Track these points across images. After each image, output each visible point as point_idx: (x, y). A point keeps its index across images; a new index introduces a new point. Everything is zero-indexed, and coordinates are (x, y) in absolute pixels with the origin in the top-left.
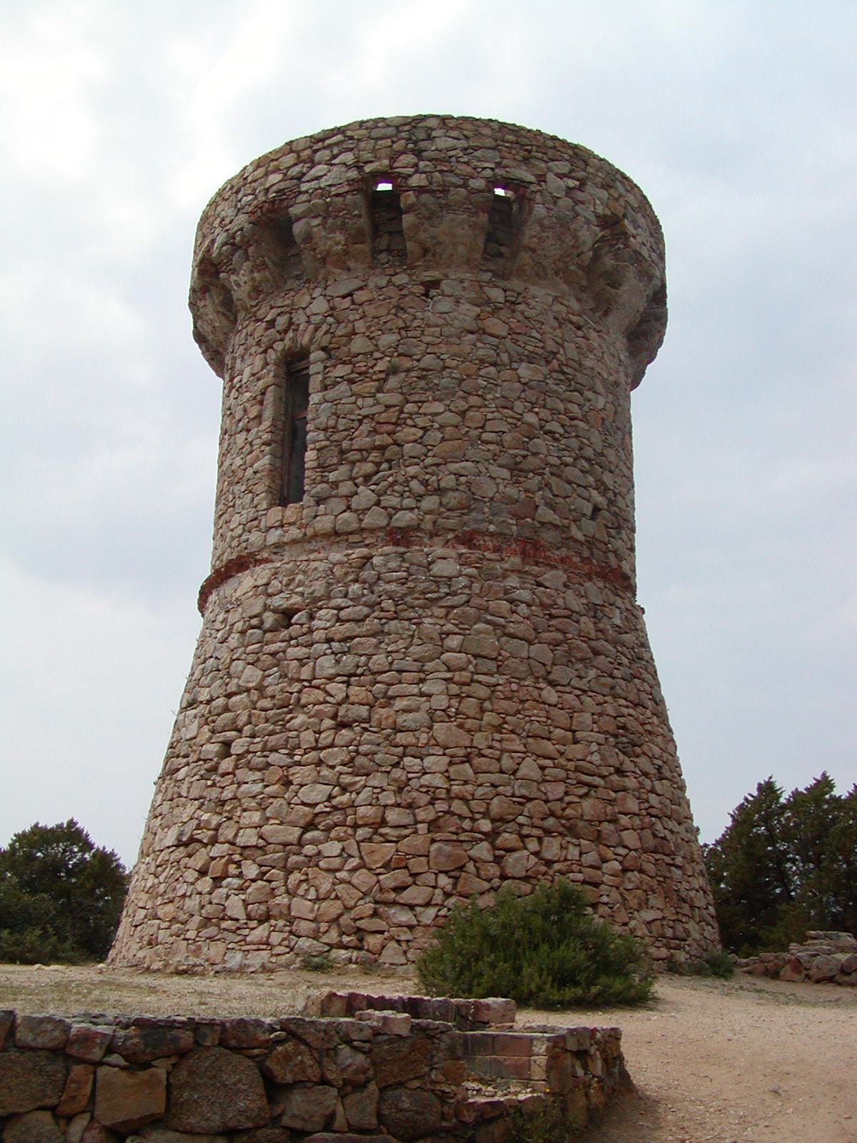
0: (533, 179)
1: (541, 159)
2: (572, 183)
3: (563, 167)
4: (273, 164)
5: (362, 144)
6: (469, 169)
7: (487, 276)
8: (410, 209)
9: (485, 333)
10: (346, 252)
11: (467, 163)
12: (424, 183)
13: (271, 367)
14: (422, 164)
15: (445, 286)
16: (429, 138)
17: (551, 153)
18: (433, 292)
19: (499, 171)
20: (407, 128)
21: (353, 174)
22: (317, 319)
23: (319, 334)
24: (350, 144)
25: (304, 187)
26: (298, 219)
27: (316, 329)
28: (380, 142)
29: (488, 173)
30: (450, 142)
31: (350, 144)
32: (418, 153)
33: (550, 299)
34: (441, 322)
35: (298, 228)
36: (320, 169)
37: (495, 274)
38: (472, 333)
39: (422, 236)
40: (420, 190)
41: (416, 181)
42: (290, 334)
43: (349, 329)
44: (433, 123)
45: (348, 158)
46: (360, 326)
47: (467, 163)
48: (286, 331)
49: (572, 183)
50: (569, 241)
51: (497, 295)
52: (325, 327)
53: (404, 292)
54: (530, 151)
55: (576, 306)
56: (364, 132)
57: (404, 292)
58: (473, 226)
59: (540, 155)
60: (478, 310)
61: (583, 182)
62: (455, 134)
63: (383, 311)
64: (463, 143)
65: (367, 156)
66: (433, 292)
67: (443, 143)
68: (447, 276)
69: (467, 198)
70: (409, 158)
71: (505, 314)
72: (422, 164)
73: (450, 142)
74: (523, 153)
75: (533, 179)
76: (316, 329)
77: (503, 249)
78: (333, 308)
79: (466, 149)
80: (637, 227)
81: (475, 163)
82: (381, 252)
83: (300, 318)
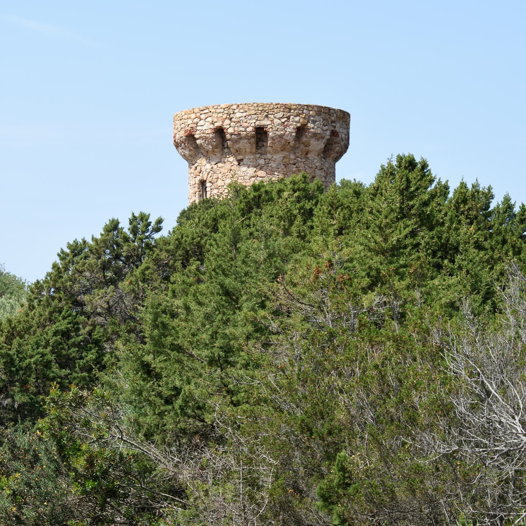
0: (269, 122)
1: (272, 114)
2: (283, 120)
3: (280, 115)
4: (189, 115)
5: (214, 115)
6: (246, 125)
7: (258, 156)
8: (229, 140)
9: (258, 176)
10: (213, 151)
11: (246, 122)
12: (232, 131)
13: (197, 185)
14: (232, 124)
15: (245, 161)
16: (234, 113)
17: (276, 110)
18: (241, 163)
19: (257, 123)
20: (227, 109)
21: (212, 126)
22: (208, 171)
23: (209, 176)
24: (210, 114)
25: (198, 128)
26: (198, 139)
27: (208, 174)
28: (219, 114)
29: (253, 124)
30: (240, 115)
31: (210, 114)
32: (231, 119)
33: (282, 158)
34: (243, 175)
35: (198, 142)
36: (201, 123)
37: (261, 154)
38: (253, 177)
39: (235, 147)
40: (231, 134)
41: (230, 130)
42: (201, 174)
43: (217, 177)
44: (235, 107)
45: (210, 119)
46: (220, 176)
47: (246, 122)
48: (200, 173)
49: (283, 120)
50: (283, 141)
51: (262, 162)
52: (210, 175)
53: (232, 164)
54: (268, 113)
55: (292, 157)
56: (214, 110)
57: (232, 164)
58: (250, 143)
59: (271, 113)
60: (255, 169)
61: (288, 118)
62: (242, 111)
63: (226, 171)
64: (245, 114)
65: (215, 120)
66: (241, 163)
67: (238, 115)
68: (245, 158)
69: (246, 135)
70: (227, 122)
71: (265, 167)
72: (232, 124)
73: (240, 115)
74: (266, 114)
75: (269, 122)
76: (208, 174)
77: (264, 144)
78: (212, 168)
79: (245, 116)
80: (314, 122)
81: (248, 121)
82: (225, 148)
83: (203, 169)
